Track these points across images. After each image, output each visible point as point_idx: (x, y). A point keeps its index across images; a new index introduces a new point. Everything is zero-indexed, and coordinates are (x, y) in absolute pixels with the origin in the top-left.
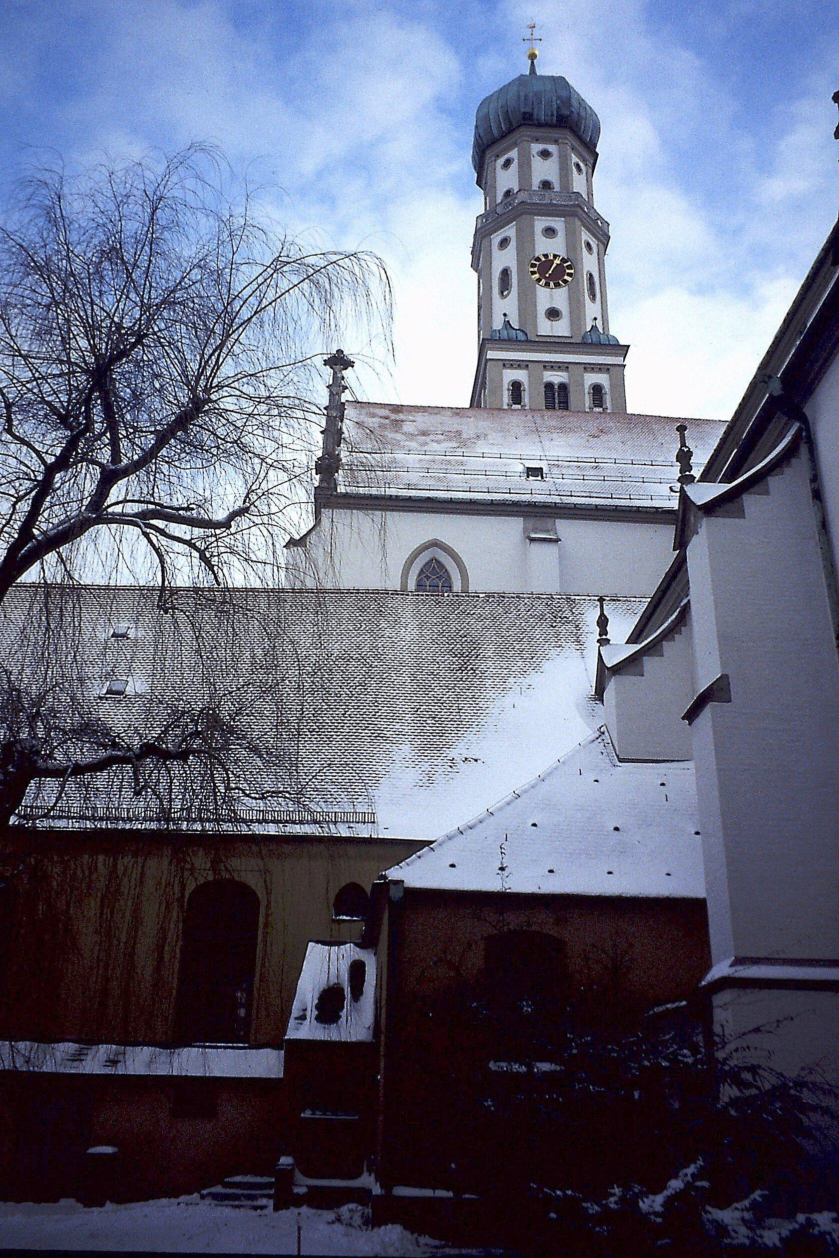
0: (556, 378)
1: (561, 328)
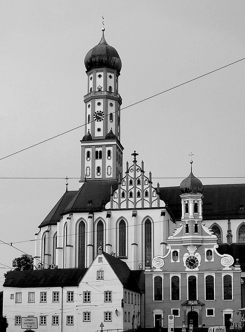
0: (99, 149)
1: (100, 134)
